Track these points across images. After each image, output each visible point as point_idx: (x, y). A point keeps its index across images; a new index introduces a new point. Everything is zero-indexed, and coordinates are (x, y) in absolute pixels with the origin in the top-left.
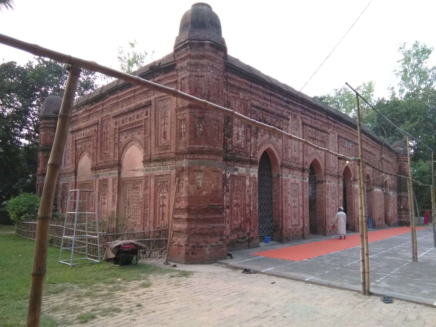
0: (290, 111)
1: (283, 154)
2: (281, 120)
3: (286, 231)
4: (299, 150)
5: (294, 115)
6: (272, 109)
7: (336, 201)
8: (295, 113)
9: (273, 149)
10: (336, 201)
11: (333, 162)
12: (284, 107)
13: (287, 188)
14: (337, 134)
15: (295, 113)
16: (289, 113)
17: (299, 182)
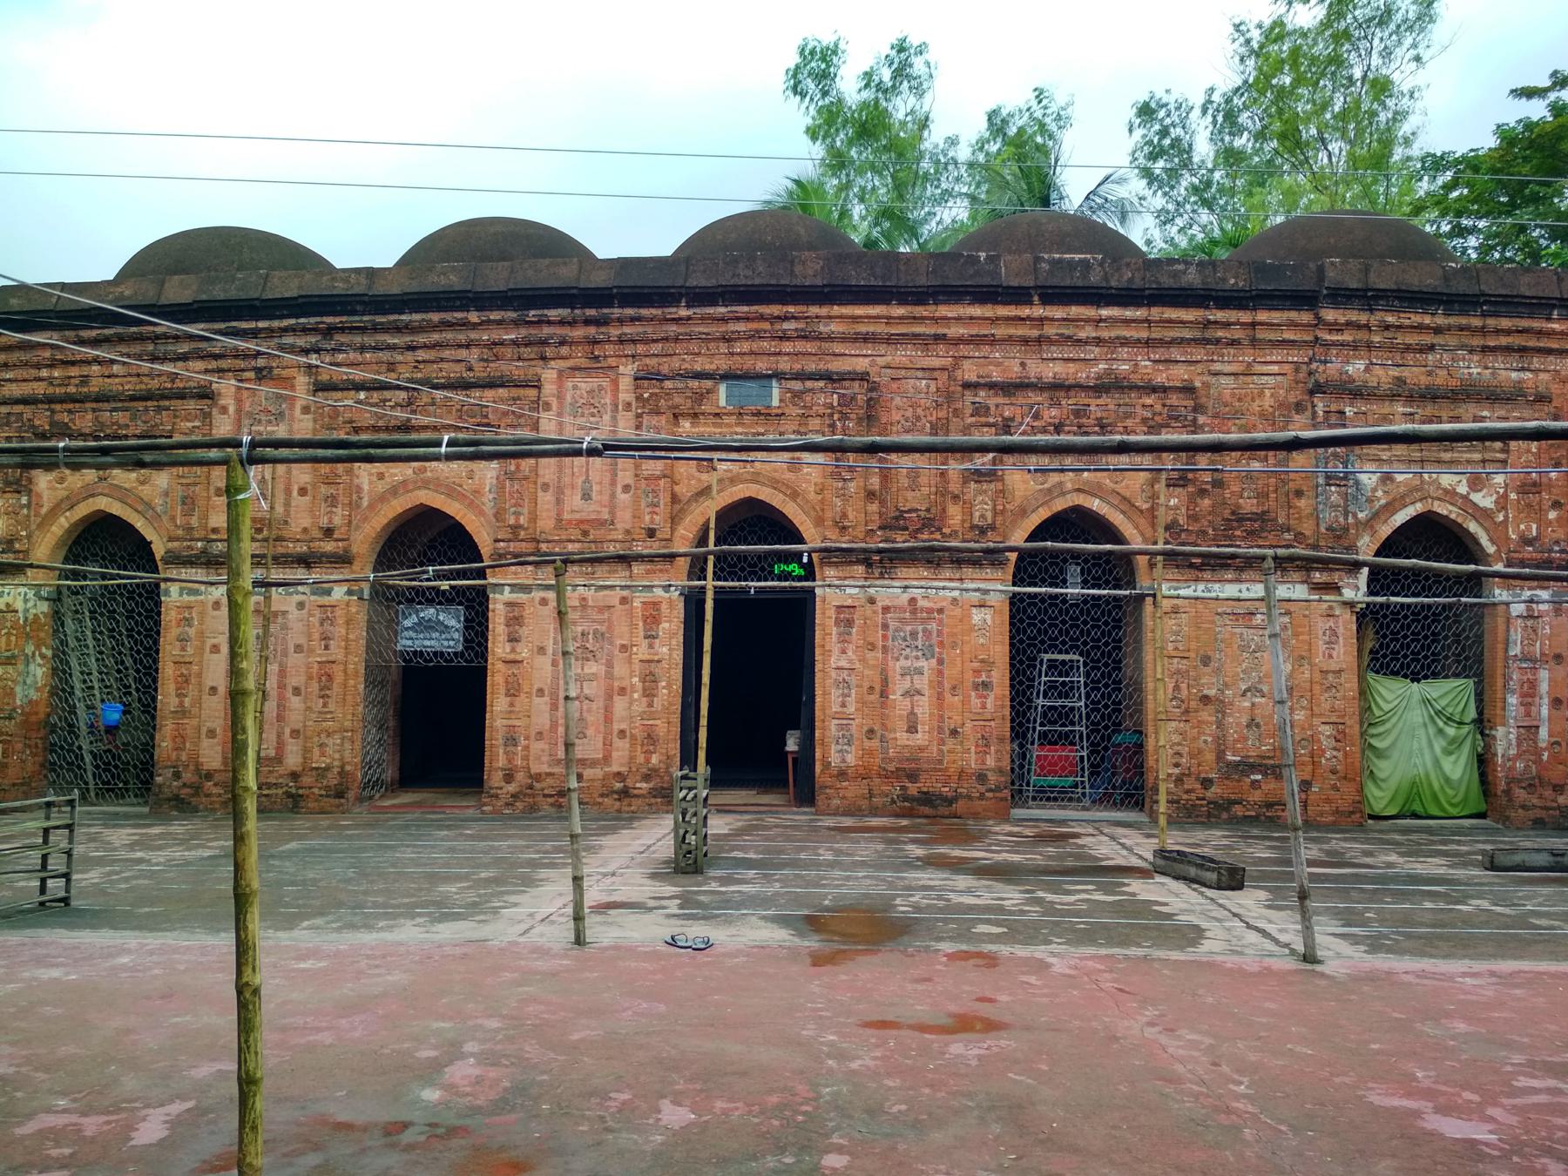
0: (224, 364)
1: (173, 518)
2: (159, 409)
3: (177, 775)
4: (288, 491)
5: (258, 370)
6: (114, 385)
7: (610, 665)
8: (261, 362)
9: (117, 509)
10: (610, 665)
11: (586, 496)
12: (184, 358)
13: (192, 632)
14: (628, 369)
15: (261, 362)
16: (220, 371)
17: (292, 608)
